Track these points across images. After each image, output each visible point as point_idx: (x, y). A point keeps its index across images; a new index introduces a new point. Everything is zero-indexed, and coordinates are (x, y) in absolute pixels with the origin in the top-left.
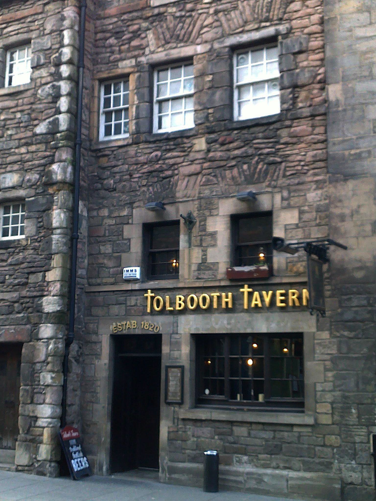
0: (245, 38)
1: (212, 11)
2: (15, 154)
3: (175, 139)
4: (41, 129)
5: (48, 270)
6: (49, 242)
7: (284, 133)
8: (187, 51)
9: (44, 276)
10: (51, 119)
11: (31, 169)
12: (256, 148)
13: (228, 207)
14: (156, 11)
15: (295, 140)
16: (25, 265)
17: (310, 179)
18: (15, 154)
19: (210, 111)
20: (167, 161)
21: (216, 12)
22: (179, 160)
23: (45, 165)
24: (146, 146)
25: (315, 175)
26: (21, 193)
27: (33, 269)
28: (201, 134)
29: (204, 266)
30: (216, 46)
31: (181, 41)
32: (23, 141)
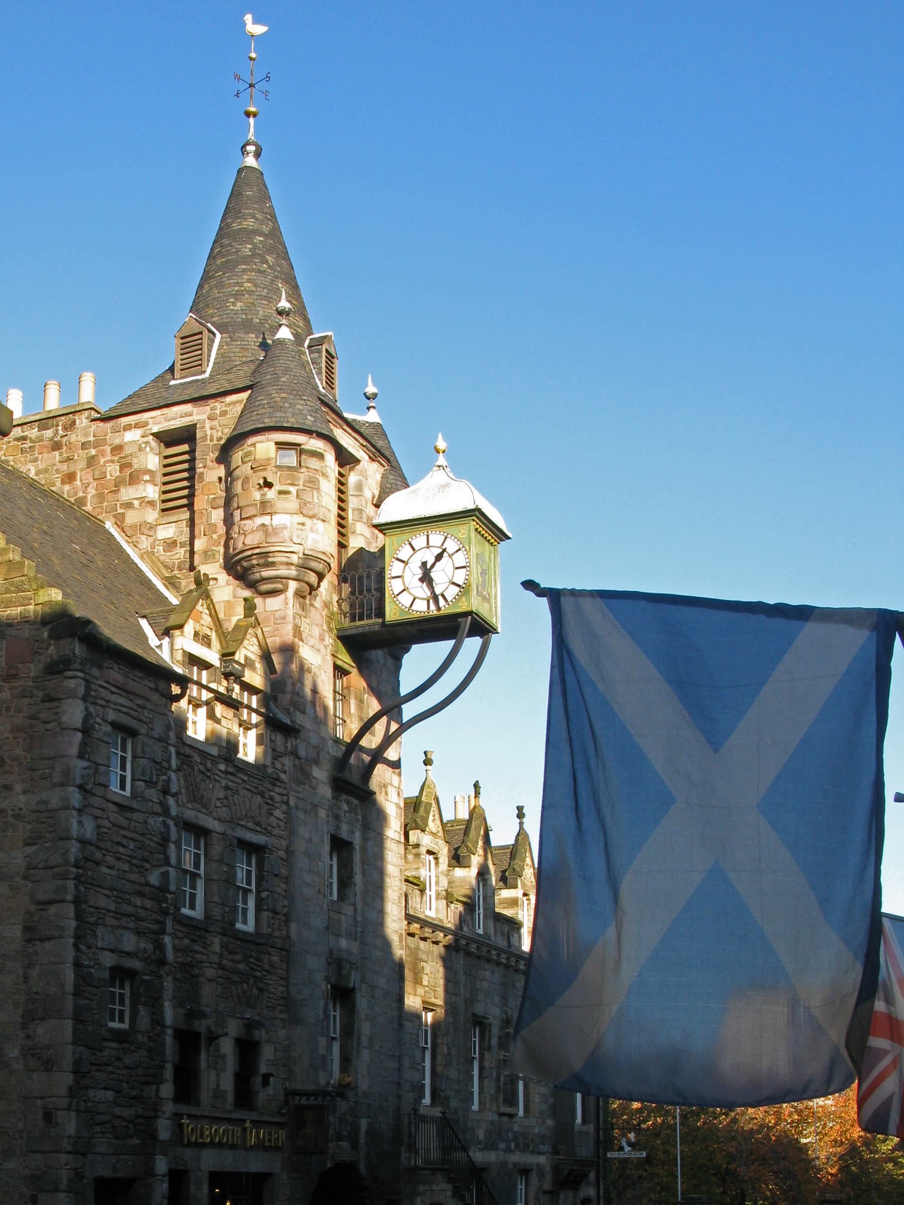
1: (223, 783)
2: (129, 903)
3: (200, 929)
4: (154, 878)
5: (162, 1083)
6: (163, 1044)
7: (266, 958)
9: (158, 1090)
10: (162, 870)
11: (144, 933)
12: (252, 969)
13: (234, 1027)
14: (188, 751)
15: (271, 970)
16: (140, 1071)
17: (278, 1015)
18: (129, 903)
19: (227, 909)
20: (196, 956)
21: (227, 788)
22: (204, 958)
23: (156, 933)
24: (179, 928)
25: (281, 1012)
26: (137, 965)
27: (149, 1079)
28: (218, 933)
29: (218, 1094)
30: (229, 832)
31: (205, 806)
32: (136, 886)
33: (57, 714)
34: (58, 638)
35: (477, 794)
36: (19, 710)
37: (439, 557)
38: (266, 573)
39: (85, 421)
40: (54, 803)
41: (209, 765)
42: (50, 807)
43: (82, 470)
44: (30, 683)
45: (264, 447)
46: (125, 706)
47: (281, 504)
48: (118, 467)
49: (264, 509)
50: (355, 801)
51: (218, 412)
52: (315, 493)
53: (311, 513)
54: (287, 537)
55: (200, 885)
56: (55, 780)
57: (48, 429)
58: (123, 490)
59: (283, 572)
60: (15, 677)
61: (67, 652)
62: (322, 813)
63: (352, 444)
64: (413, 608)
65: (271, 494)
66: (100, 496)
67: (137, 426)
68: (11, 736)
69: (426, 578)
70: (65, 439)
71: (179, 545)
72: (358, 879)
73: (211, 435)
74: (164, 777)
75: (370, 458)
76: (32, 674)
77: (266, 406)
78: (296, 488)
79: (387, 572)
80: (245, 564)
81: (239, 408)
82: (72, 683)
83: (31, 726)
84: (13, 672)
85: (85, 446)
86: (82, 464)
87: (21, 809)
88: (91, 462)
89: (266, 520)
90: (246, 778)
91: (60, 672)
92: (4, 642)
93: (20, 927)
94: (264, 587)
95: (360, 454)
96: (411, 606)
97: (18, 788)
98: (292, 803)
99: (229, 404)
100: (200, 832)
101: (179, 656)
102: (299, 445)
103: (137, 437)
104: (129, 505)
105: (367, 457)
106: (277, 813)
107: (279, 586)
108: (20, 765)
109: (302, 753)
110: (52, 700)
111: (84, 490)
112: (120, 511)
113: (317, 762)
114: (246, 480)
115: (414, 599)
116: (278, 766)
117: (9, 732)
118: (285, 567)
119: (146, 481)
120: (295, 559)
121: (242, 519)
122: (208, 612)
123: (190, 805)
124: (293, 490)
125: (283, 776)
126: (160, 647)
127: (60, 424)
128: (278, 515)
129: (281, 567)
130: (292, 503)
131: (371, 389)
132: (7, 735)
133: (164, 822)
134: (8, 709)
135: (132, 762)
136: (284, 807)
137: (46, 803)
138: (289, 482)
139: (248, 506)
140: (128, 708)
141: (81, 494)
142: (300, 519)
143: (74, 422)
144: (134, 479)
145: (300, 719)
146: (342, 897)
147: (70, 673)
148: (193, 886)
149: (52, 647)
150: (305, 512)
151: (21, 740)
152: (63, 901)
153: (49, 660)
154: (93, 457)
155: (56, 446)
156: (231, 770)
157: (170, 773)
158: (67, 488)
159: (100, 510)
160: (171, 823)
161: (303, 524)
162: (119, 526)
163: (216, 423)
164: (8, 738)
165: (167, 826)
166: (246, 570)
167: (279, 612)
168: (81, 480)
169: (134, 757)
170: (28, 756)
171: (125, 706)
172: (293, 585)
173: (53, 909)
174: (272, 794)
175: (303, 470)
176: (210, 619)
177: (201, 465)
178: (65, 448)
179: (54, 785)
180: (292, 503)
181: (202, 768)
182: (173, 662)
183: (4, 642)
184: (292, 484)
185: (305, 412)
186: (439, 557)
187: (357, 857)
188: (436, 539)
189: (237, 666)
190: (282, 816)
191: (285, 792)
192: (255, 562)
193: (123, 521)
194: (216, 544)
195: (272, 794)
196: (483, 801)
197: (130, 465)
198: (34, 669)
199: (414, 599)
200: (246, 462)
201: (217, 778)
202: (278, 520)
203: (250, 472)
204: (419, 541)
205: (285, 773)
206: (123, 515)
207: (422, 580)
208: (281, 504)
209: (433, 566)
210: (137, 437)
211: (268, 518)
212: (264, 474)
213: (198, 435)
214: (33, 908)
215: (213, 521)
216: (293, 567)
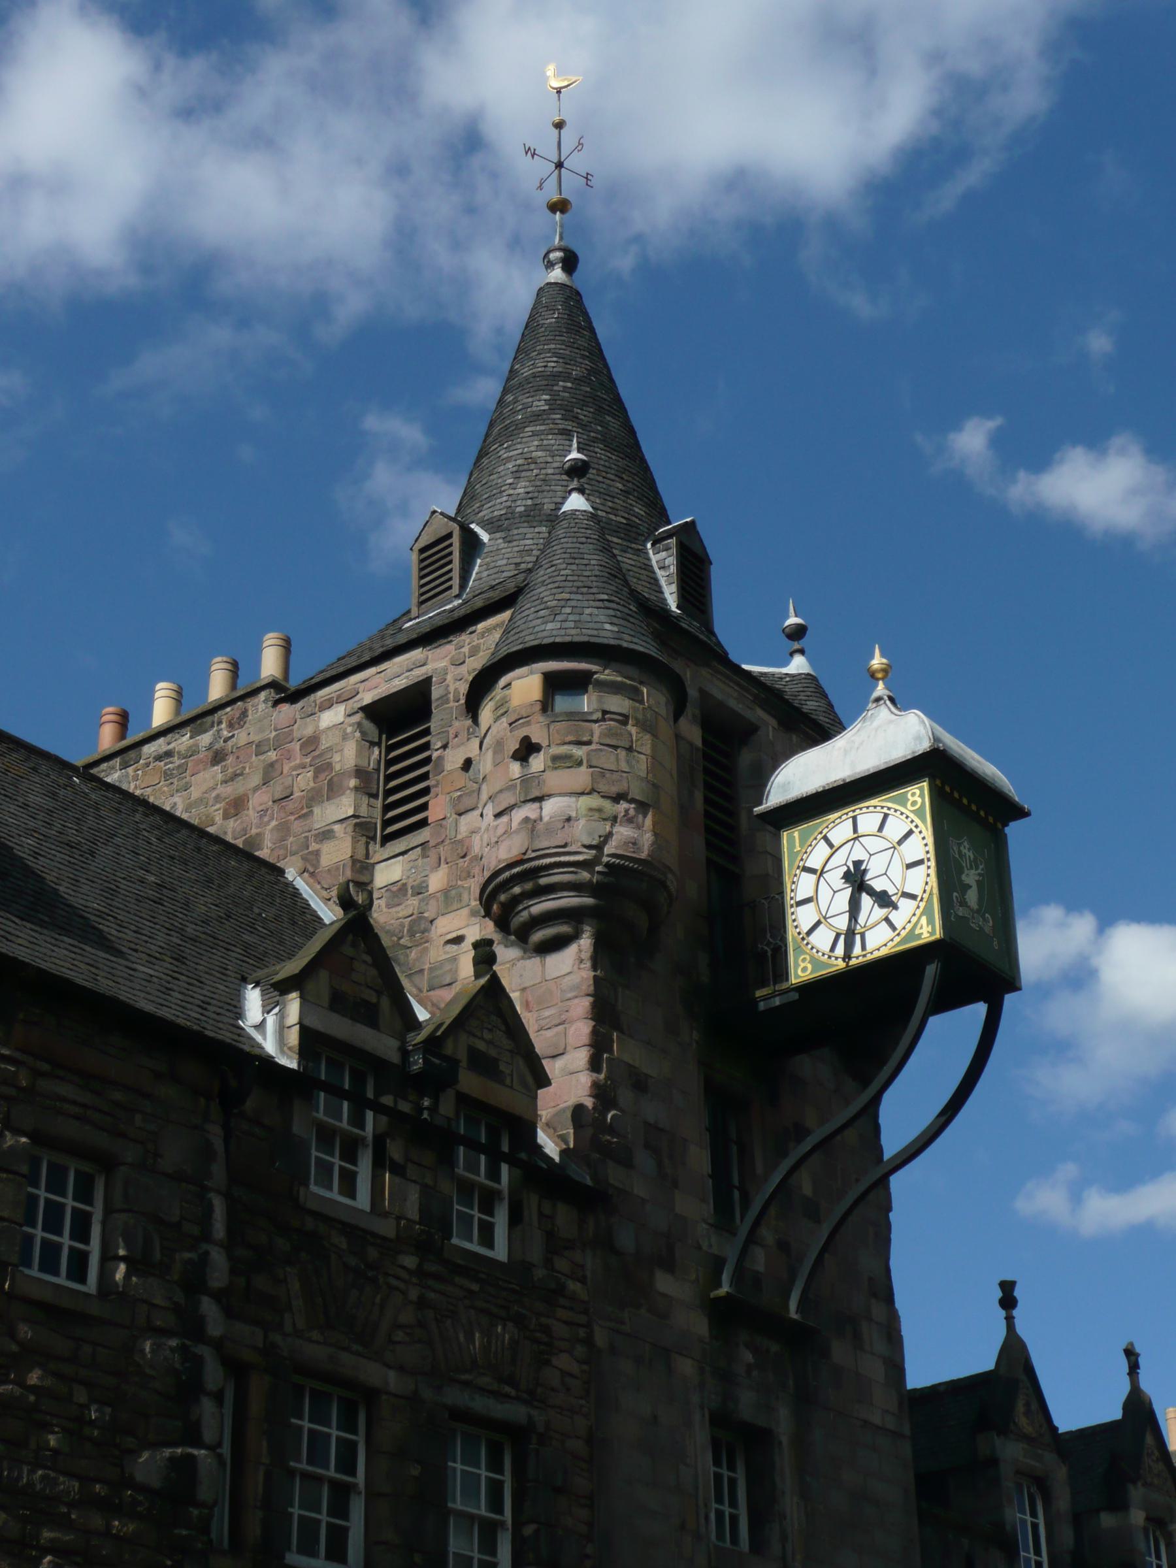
0: (480, 1404)
1: (414, 1294)
8: (372, 1373)
35: (1134, 1368)
38: (540, 907)
39: (262, 706)
41: (373, 1253)
43: (256, 789)
45: (525, 685)
46: (74, 1103)
48: (310, 774)
50: (775, 1348)
51: (466, 650)
52: (622, 754)
53: (614, 790)
55: (357, 1508)
57: (206, 731)
58: (317, 810)
59: (569, 900)
62: (686, 1367)
63: (735, 695)
65: (537, 762)
66: (284, 829)
67: (341, 700)
70: (230, 743)
71: (410, 892)
72: (790, 1505)
73: (456, 689)
74: (187, 1255)
75: (780, 723)
78: (585, 748)
79: (788, 894)
81: (497, 635)
85: (260, 748)
86: (256, 780)
88: (269, 773)
89: (529, 811)
90: (475, 1287)
94: (538, 936)
95: (759, 715)
98: (601, 1338)
99: (482, 635)
100: (358, 1400)
101: (293, 1037)
103: (334, 718)
104: (326, 835)
105: (773, 722)
106: (563, 1361)
107: (564, 929)
109: (626, 1239)
111: (257, 826)
112: (314, 846)
113: (669, 1264)
116: (562, 1264)
119: (356, 789)
122: (368, 959)
123: (315, 1335)
124: (579, 752)
125: (573, 1286)
126: (261, 1026)
127: (224, 719)
129: (566, 894)
131: (793, 620)
133: (183, 1349)
135: (104, 1223)
136: (580, 1350)
138: (570, 738)
139: (501, 791)
140: (85, 1106)
141: (254, 831)
142: (594, 801)
143: (244, 713)
144: (333, 790)
145: (615, 1175)
146: (758, 1545)
148: (340, 1508)
150: (602, 787)
154: (272, 765)
155: (218, 757)
156: (432, 1268)
157: (205, 1246)
158: (232, 824)
159: (282, 852)
160: (205, 1352)
161: (599, 810)
162: (312, 874)
165: (199, 1361)
167: (568, 978)
168: (254, 808)
169: (108, 1210)
171: (74, 1103)
174: (544, 1320)
176: (373, 972)
177: (439, 744)
178: (230, 760)
181: (352, 1261)
182: (282, 1052)
184: (579, 743)
185: (603, 619)
187: (785, 1460)
189: (437, 1061)
190: (575, 1368)
191: (583, 1319)
192: (517, 890)
193: (316, 865)
194: (464, 875)
195: (544, 1320)
196: (1145, 1385)
197: (329, 766)
201: (394, 1282)
202: (550, 807)
205: (583, 1280)
206: (317, 853)
208: (558, 779)
210: (334, 718)
211: (537, 805)
213: (436, 693)
215: (459, 837)
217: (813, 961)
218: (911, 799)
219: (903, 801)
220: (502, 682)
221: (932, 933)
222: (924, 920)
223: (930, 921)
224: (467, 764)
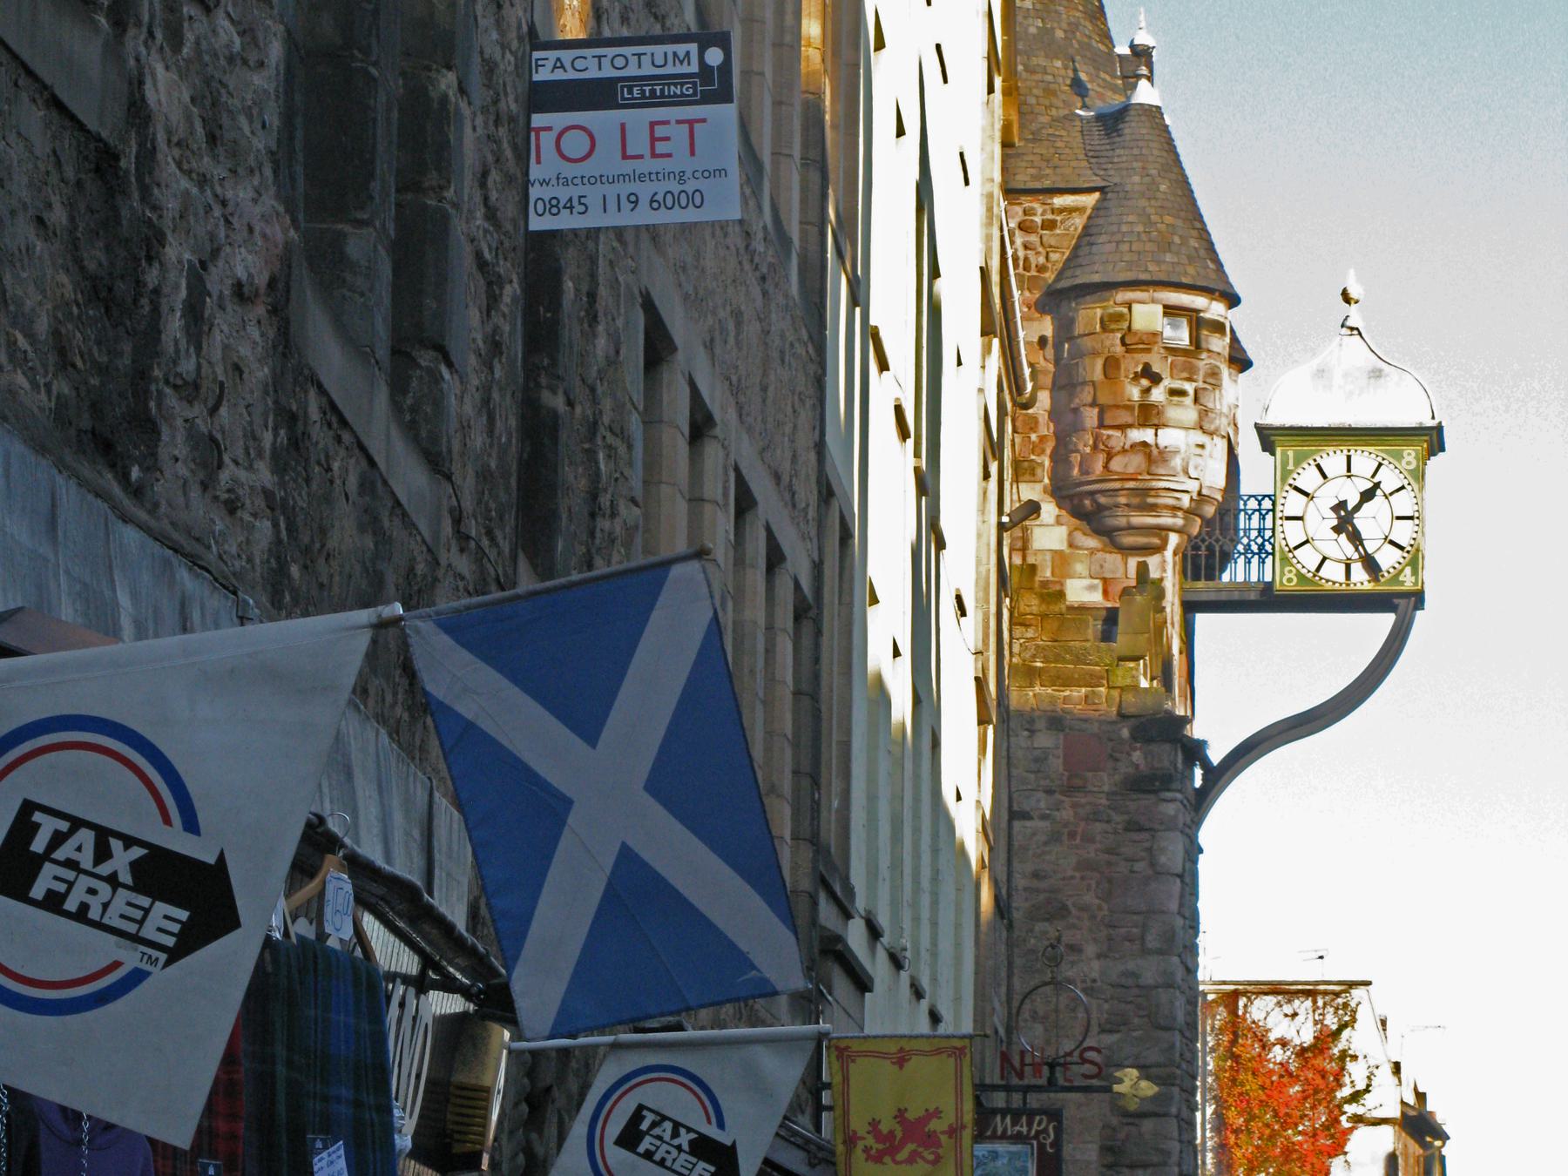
33: (1149, 850)
34: (1150, 740)
36: (1091, 840)
37: (1367, 496)
40: (1149, 977)
42: (1142, 982)
44: (1104, 801)
47: (1173, 413)
49: (1146, 419)
51: (1038, 219)
53: (1213, 428)
54: (1179, 468)
56: (1150, 946)
59: (1166, 520)
60: (1078, 789)
61: (1166, 764)
64: (1321, 573)
65: (1158, 395)
68: (1077, 875)
69: (1345, 521)
73: (1026, 259)
76: (1106, 788)
77: (1144, 237)
80: (1102, 500)
81: (1079, 222)
82: (1170, 809)
83: (1109, 864)
84: (1078, 782)
87: (1094, 981)
89: (1147, 435)
91: (1155, 792)
92: (1061, 736)
93: (1095, 1147)
96: (1318, 569)
97: (1091, 950)
99: (1061, 211)
102: (1197, 311)
107: (1156, 541)
108: (1093, 917)
110: (1141, 829)
114: (1111, 365)
115: (1324, 559)
117: (1076, 869)
118: (1169, 513)
120: (1185, 501)
121: (1101, 425)
124: (1189, 387)
128: (1167, 430)
130: (1185, 412)
132: (1070, 873)
134: (1072, 835)
137: (1134, 975)
147: (1169, 795)
149: (1138, 753)
151: (1093, 883)
152: (1165, 1115)
153: (1131, 770)
161: (1202, 446)
163: (1033, 238)
164: (1072, 878)
166: (1101, 508)
170: (1105, 906)
172: (1174, 539)
173: (1148, 1125)
175: (1204, 355)
179: (1145, 952)
180: (1185, 412)
183: (1061, 736)
184: (1190, 379)
186: (1367, 496)
188: (1364, 462)
192: (1123, 500)
198: (1105, 782)
199: (1324, 559)
200: (1113, 331)
203: (1119, 349)
204: (1333, 461)
207: (1337, 530)
209: (1357, 508)
211: (1151, 432)
212: (1145, 358)
214: (1115, 1121)
216: (1180, 514)
217: (1299, 574)
218: (1408, 458)
219: (1399, 457)
220: (1122, 296)
221: (1416, 584)
222: (1408, 570)
223: (1415, 572)
224: (1042, 341)
